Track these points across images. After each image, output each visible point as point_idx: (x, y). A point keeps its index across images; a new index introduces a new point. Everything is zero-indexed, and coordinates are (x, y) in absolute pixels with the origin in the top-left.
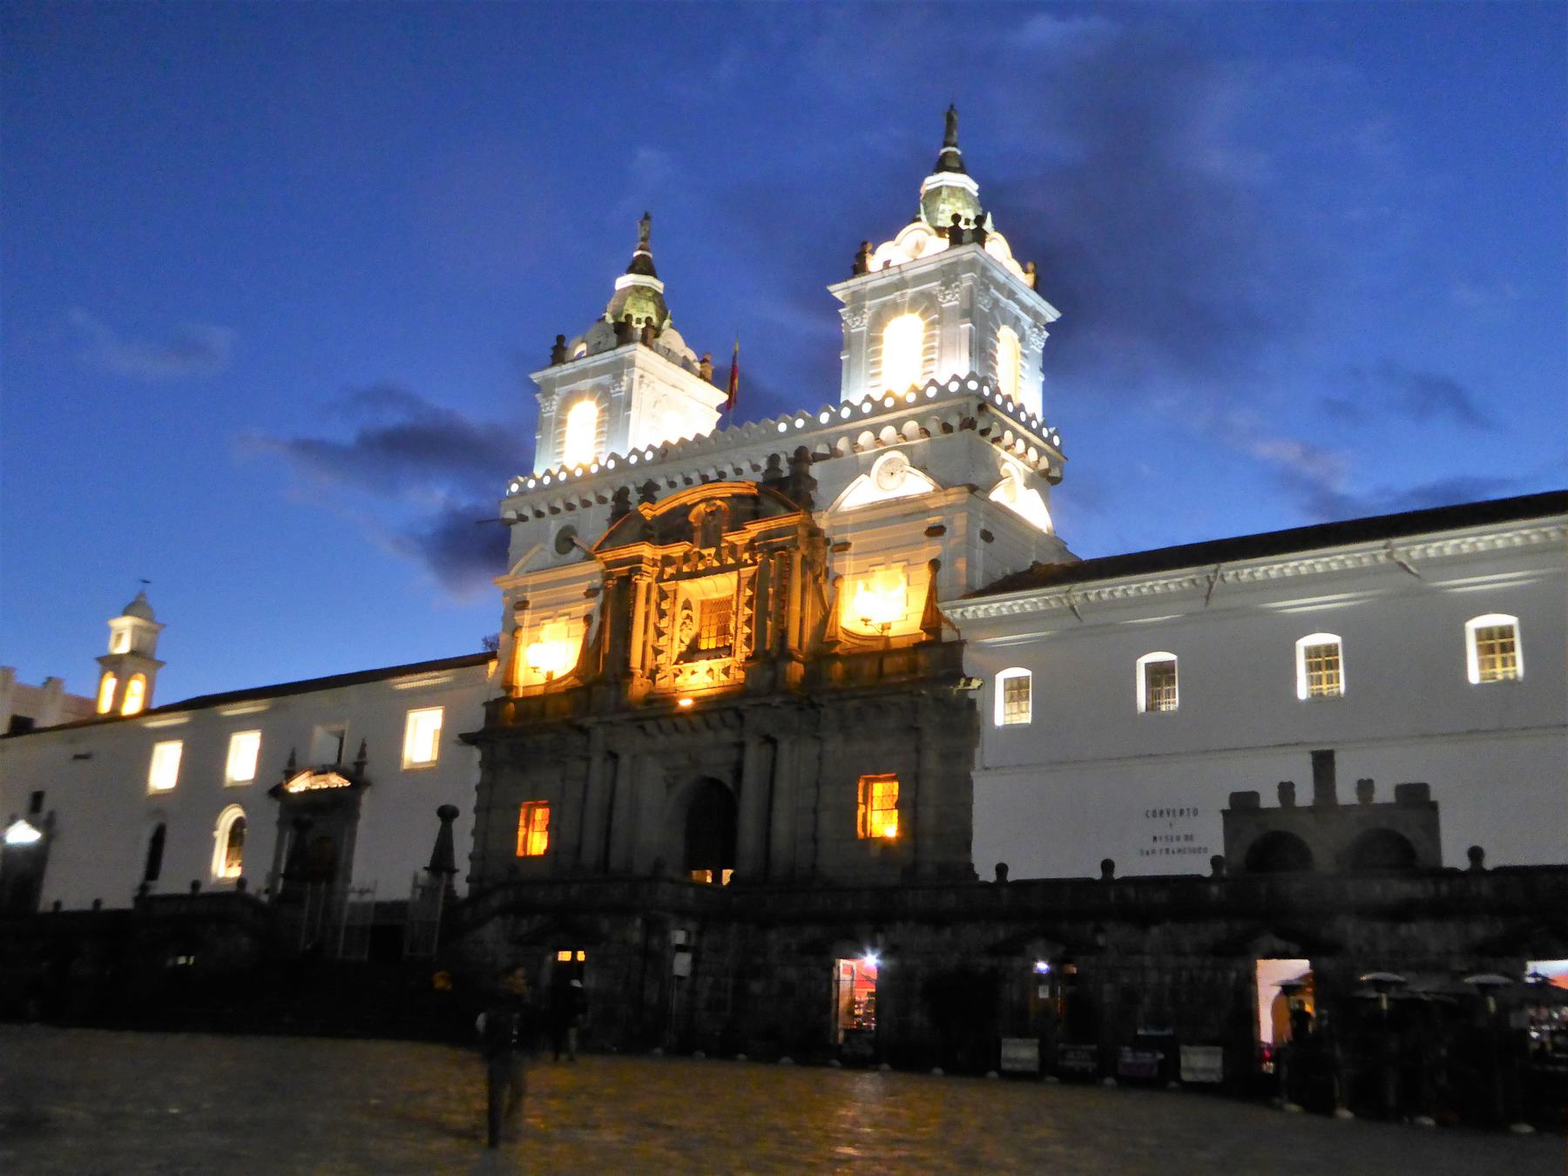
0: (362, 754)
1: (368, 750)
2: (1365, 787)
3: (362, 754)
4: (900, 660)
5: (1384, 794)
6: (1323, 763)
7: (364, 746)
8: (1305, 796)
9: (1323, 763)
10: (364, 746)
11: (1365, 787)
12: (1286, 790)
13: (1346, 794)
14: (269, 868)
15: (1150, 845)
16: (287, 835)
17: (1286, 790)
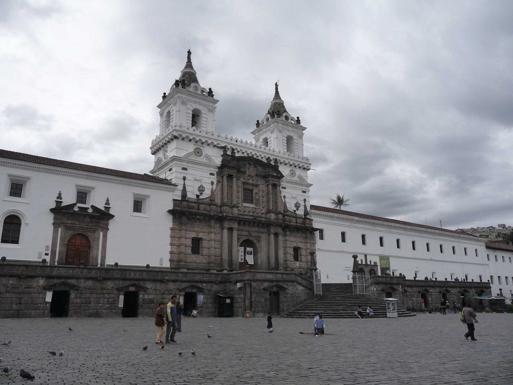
0: (107, 203)
1: (110, 202)
2: (370, 262)
3: (107, 203)
4: (301, 220)
5: (372, 264)
6: (366, 256)
7: (108, 200)
8: (364, 263)
9: (366, 256)
10: (108, 200)
11: (370, 262)
12: (362, 260)
13: (369, 263)
14: (50, 244)
15: (345, 269)
16: (60, 229)
17: (362, 260)
